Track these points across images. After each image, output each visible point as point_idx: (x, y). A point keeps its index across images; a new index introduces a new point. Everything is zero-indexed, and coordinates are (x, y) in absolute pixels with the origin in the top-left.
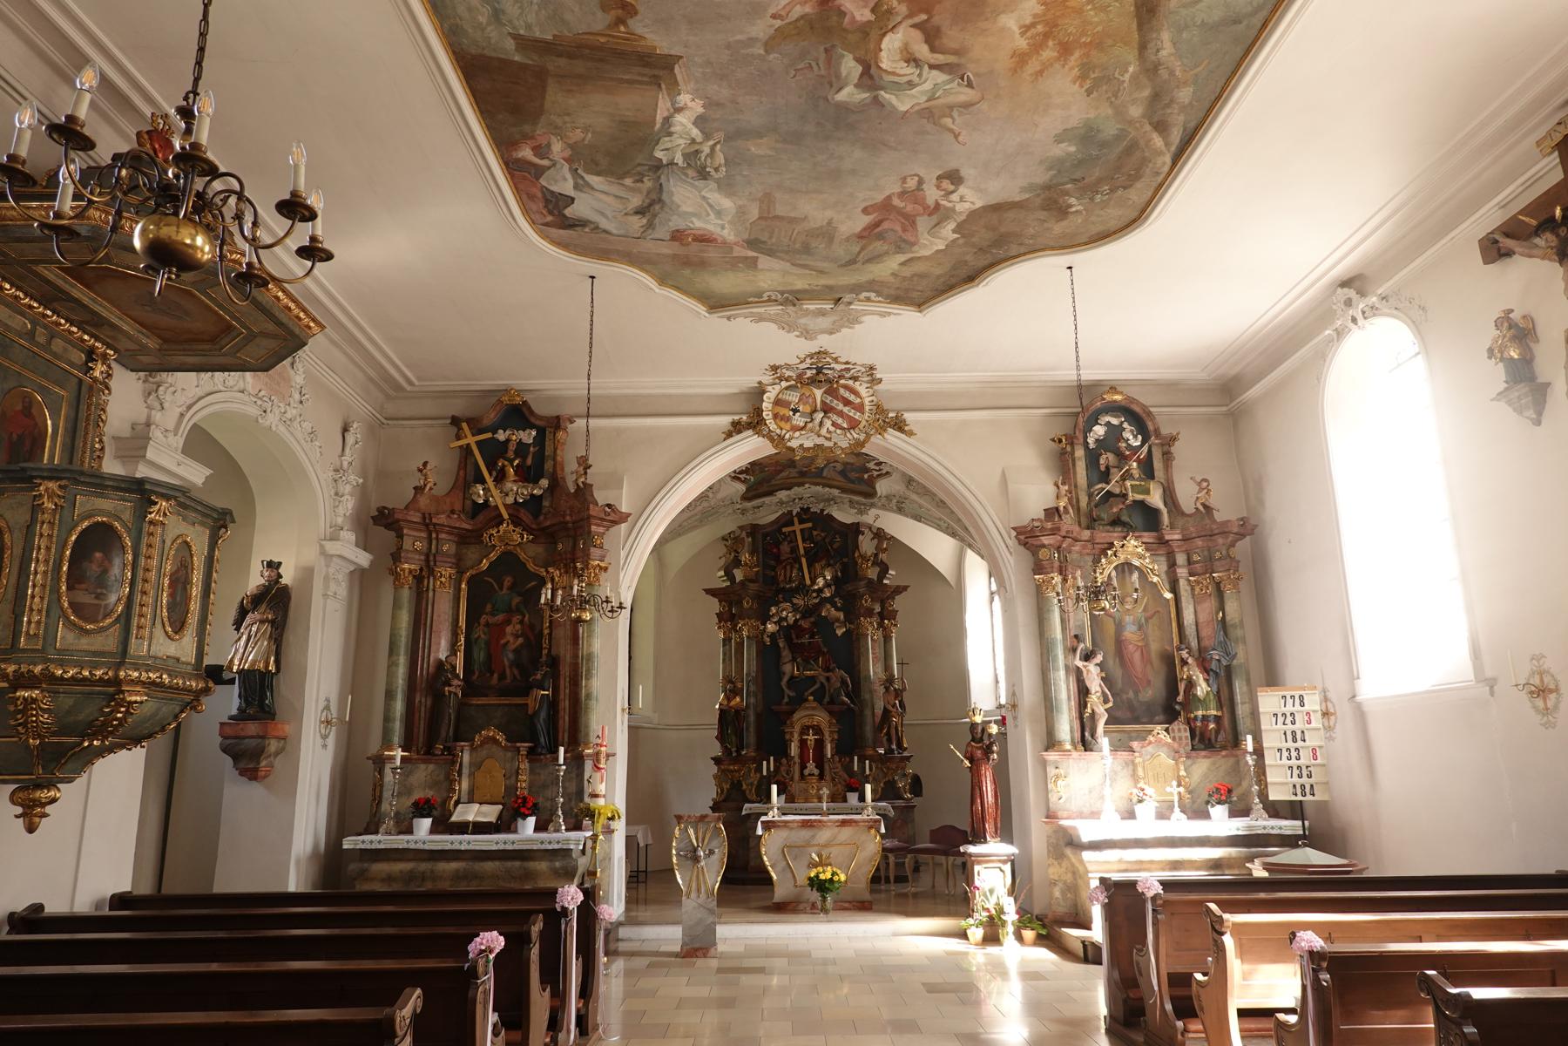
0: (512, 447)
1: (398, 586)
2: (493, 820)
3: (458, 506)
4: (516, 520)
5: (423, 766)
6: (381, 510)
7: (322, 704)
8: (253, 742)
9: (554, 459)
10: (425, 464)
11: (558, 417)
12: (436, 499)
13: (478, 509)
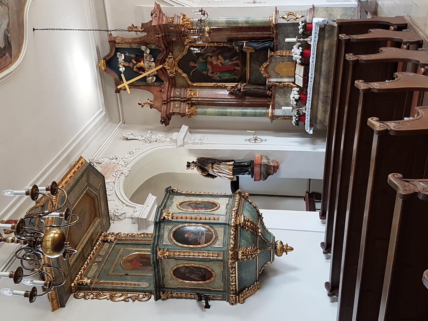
0: (127, 64)
1: (196, 113)
2: (302, 68)
3: (158, 89)
4: (163, 61)
5: (276, 99)
6: (162, 122)
7: (248, 142)
8: (263, 169)
9: (131, 43)
10: (140, 104)
11: (109, 42)
12: (156, 98)
13: (158, 80)
